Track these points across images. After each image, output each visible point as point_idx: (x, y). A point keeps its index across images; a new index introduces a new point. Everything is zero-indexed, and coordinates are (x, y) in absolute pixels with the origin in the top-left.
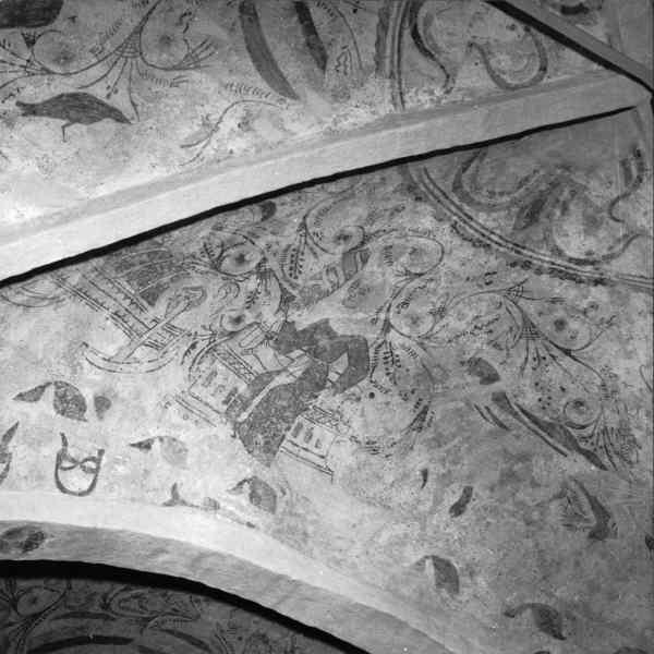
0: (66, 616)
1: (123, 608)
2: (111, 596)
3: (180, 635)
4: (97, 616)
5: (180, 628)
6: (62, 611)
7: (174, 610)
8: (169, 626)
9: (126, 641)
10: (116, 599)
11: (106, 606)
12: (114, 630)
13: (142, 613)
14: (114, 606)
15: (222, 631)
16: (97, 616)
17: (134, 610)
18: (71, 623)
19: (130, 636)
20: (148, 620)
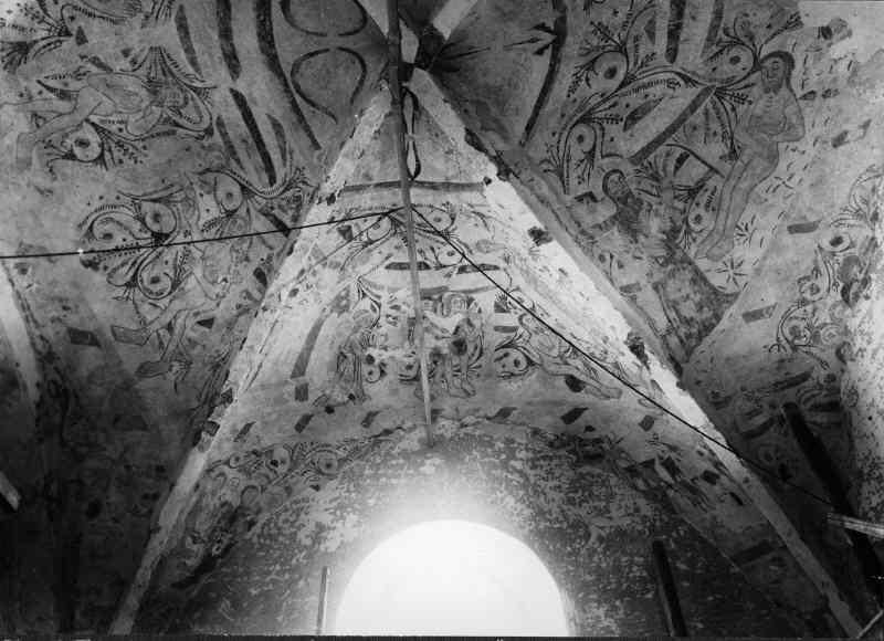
0: (238, 161)
1: (201, 117)
2: (195, 134)
3: (189, 50)
4: (224, 135)
5: (182, 57)
6: (234, 164)
7: (164, 74)
8: (190, 70)
9: (237, 96)
10: (196, 127)
11: (209, 132)
12: (233, 114)
13: (192, 99)
14: (205, 125)
15: (147, 17)
16: (224, 135)
17: (197, 107)
18: (242, 154)
19: (228, 93)
20: (195, 89)
